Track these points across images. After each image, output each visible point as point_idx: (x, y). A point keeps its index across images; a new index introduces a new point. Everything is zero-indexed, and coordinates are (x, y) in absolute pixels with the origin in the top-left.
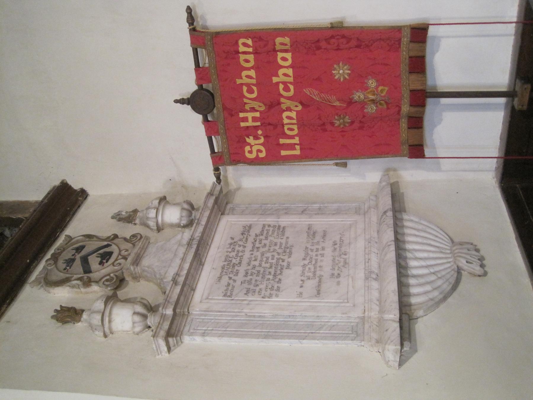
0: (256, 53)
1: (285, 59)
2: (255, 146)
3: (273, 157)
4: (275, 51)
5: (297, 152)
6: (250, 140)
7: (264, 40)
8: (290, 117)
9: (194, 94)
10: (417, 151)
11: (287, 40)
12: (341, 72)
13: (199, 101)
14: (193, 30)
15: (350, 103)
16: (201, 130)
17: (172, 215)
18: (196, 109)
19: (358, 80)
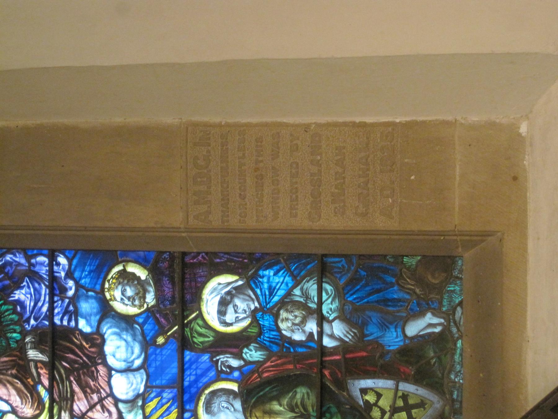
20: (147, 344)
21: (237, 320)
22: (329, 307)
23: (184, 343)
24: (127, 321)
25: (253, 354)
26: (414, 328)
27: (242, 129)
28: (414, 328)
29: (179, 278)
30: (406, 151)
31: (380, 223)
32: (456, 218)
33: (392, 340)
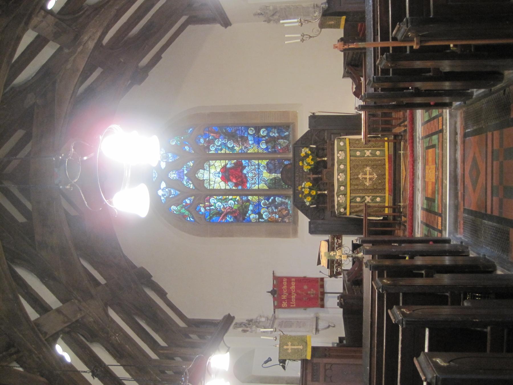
0: (287, 282)
1: (293, 284)
2: (285, 304)
3: (289, 307)
4: (291, 282)
5: (295, 306)
6: (284, 302)
7: (289, 279)
8: (293, 297)
9: (272, 291)
10: (322, 306)
11: (294, 279)
12: (305, 287)
13: (273, 292)
14: (274, 276)
15: (307, 294)
16: (272, 299)
17: (263, 319)
18: (272, 294)
19: (309, 289)
20: (254, 137)
21: (265, 134)
22: (276, 132)
23: (258, 137)
24: (251, 135)
25: (267, 138)
26: (285, 134)
27: (267, 112)
28: (285, 134)
29: (258, 129)
30: (285, 114)
31: (282, 122)
32: (290, 121)
33: (283, 136)
